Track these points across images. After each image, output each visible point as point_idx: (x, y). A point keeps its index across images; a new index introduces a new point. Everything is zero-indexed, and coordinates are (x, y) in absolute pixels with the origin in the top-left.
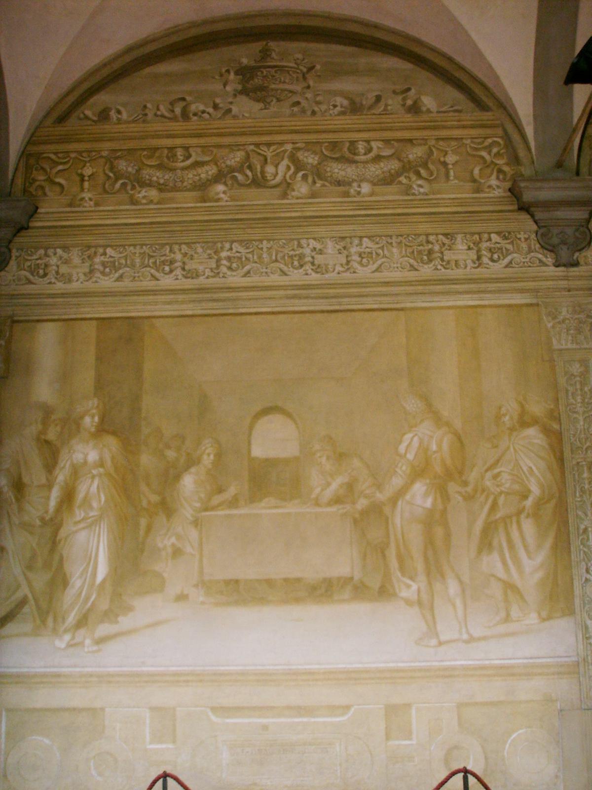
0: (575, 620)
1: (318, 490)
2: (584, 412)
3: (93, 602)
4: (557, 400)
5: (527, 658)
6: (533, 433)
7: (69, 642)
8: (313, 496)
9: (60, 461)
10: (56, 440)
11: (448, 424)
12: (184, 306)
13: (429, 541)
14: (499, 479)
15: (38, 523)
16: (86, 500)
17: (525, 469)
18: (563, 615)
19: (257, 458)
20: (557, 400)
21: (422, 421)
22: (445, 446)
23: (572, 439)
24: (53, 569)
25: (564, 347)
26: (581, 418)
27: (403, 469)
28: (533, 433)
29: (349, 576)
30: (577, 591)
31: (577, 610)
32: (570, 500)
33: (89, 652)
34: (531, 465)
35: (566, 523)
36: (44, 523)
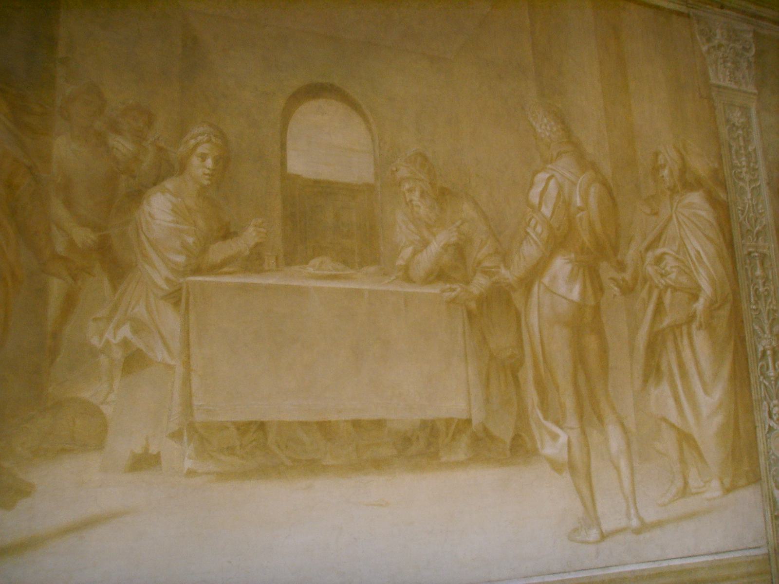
0: (762, 490)
1: (408, 252)
2: (751, 181)
4: (720, 157)
5: (712, 554)
6: (696, 198)
8: (400, 262)
11: (594, 167)
13: (579, 359)
14: (662, 265)
17: (692, 253)
18: (749, 483)
19: (298, 176)
20: (720, 157)
21: (559, 154)
22: (593, 201)
23: (741, 218)
25: (722, 83)
26: (748, 189)
27: (537, 231)
28: (696, 198)
29: (465, 416)
30: (761, 447)
31: (763, 474)
32: (744, 305)
34: (699, 248)
35: (743, 340)
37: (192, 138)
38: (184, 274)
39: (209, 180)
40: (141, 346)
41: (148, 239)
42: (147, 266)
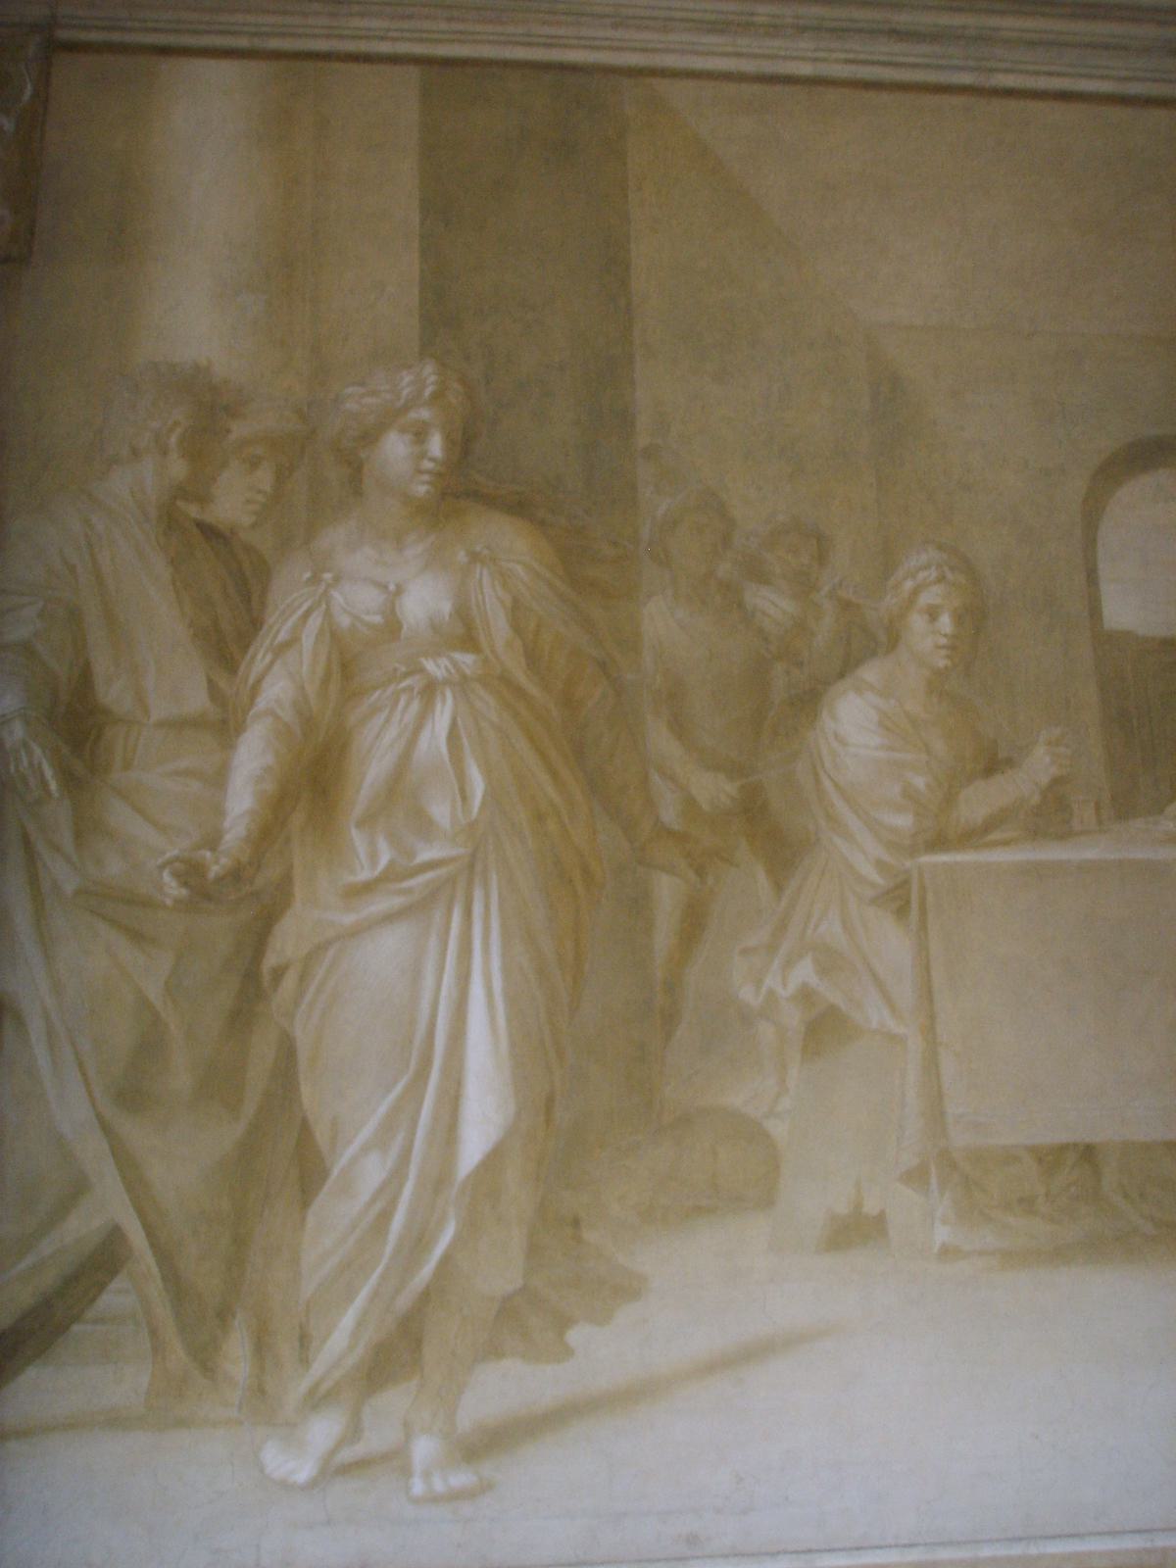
3: (446, 1260)
7: (333, 1452)
9: (272, 618)
10: (254, 526)
12: (775, 45)
15: (173, 889)
16: (398, 788)
19: (1127, 634)
24: (249, 1109)
33: (435, 1499)
36: (200, 888)
37: (905, 579)
38: (913, 851)
39: (948, 657)
40: (835, 997)
41: (836, 785)
42: (838, 841)
